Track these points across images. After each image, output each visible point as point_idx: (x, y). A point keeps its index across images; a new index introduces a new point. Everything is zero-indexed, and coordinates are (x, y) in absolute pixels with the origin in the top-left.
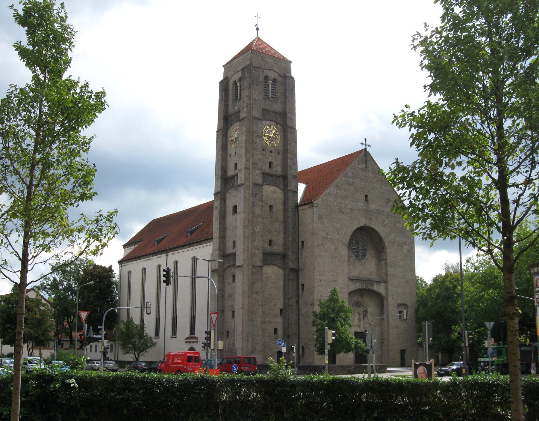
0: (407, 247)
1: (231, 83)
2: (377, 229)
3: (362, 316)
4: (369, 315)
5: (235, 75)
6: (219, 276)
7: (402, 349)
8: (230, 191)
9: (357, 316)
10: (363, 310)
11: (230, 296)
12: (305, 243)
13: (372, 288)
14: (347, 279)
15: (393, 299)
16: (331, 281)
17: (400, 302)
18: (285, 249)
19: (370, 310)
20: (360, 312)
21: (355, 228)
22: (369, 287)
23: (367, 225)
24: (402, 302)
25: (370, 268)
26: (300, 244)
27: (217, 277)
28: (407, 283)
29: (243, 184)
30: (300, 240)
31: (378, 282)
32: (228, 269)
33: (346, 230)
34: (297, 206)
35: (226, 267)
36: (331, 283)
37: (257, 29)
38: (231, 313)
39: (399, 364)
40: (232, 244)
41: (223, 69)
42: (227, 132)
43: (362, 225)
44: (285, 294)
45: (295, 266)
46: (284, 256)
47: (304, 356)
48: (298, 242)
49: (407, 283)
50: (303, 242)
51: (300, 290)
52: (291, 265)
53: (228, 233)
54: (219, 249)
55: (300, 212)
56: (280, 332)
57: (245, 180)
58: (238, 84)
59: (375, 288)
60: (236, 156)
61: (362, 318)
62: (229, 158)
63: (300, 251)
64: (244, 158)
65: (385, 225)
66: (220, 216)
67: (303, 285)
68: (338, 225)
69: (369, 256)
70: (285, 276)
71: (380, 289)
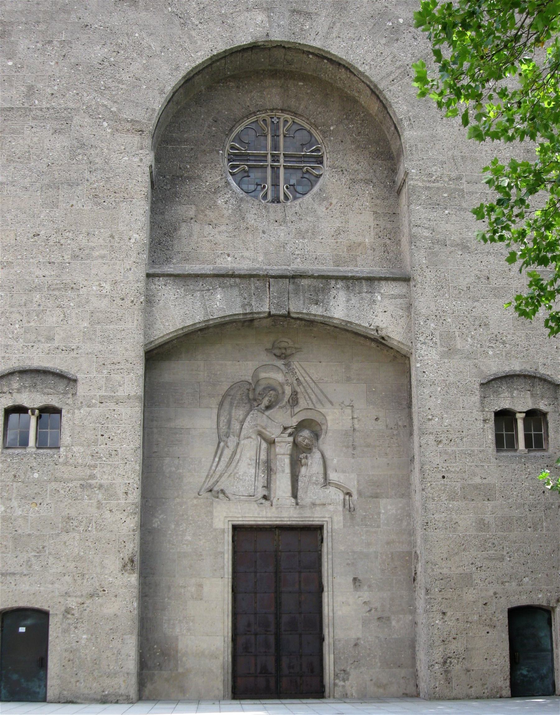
2: (337, 49)
3: (283, 449)
4: (329, 445)
7: (524, 601)
9: (249, 450)
10: (294, 422)
13: (316, 310)
15: (450, 352)
17: (495, 366)
19: (335, 420)
20: (274, 432)
21: (200, 57)
22: (297, 306)
23: (277, 36)
24: (516, 366)
25: (338, 232)
31: (351, 281)
33: (146, 68)
36: (37, 297)
39: (503, 681)
43: (244, 39)
59: (340, 307)
61: (283, 463)
68: (99, 52)
69: (329, 179)
71: (381, 314)
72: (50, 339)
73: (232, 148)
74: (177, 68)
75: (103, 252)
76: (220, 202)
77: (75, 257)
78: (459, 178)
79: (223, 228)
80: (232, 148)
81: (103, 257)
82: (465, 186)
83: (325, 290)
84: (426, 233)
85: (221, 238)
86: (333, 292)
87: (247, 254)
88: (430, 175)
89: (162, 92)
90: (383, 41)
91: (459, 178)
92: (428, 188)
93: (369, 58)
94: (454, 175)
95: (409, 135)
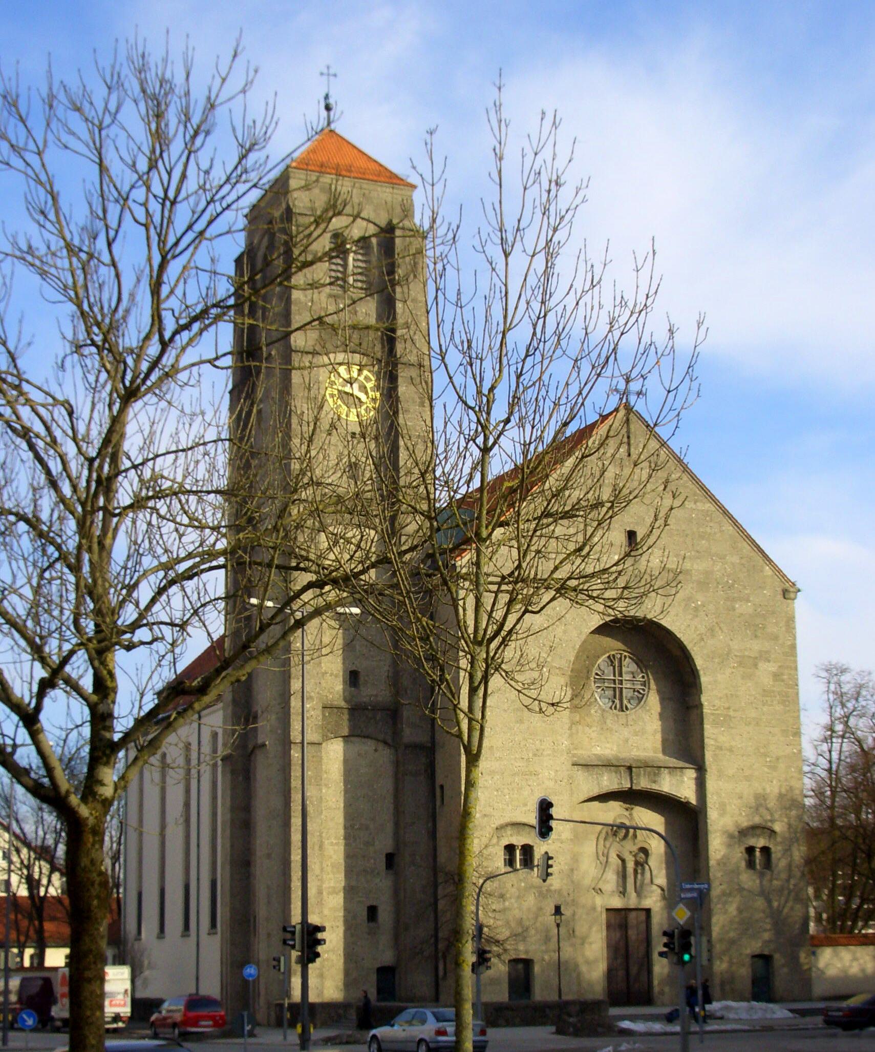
0: (772, 667)
13: (655, 787)
14: (568, 765)
16: (514, 775)
18: (397, 694)
28: (774, 768)
33: (565, 632)
37: (328, 108)
44: (398, 811)
45: (422, 738)
46: (393, 713)
49: (774, 768)
51: (438, 803)
52: (409, 734)
56: (385, 916)
65: (696, 609)
67: (442, 787)
70: (397, 764)
72: (525, 805)
73: (597, 674)
74: (581, 633)
75: (549, 752)
76: (592, 711)
77: (535, 755)
78: (729, 708)
79: (595, 729)
80: (597, 674)
81: (549, 755)
82: (731, 713)
83: (658, 774)
84: (712, 742)
85: (594, 735)
86: (663, 776)
87: (608, 745)
88: (714, 706)
89: (573, 647)
90: (690, 617)
91: (729, 708)
92: (713, 714)
93: (683, 627)
94: (727, 705)
95: (704, 680)
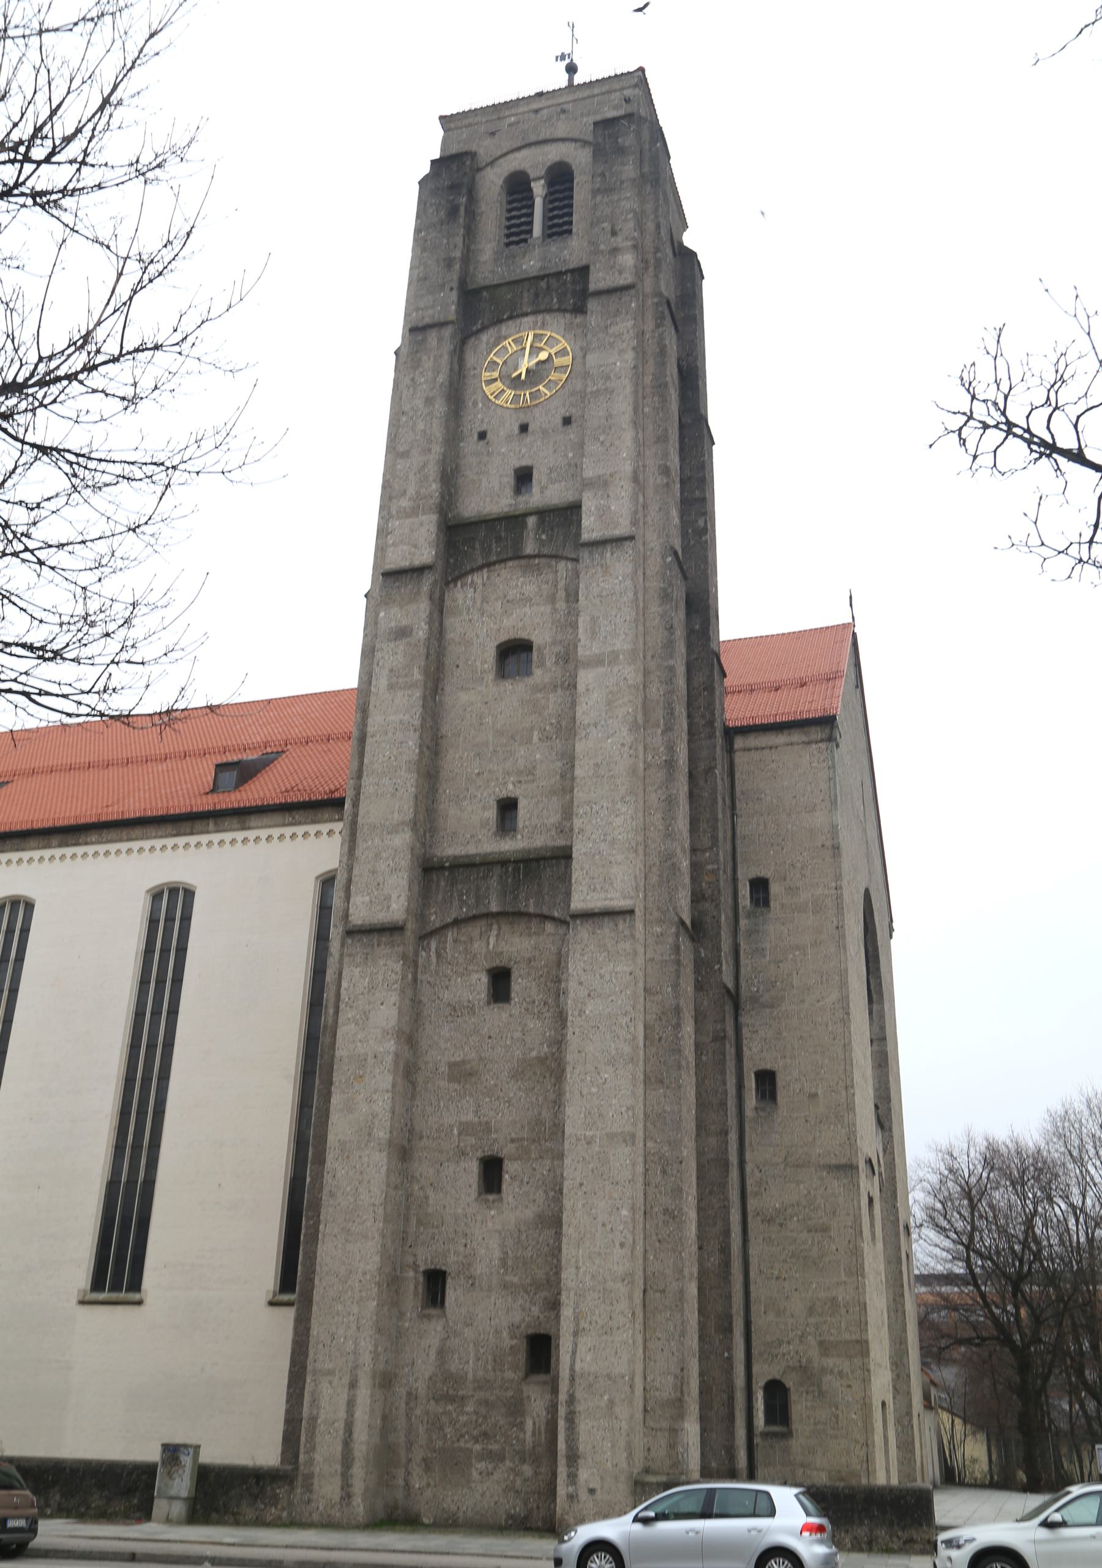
1: (492, 182)
5: (525, 152)
6: (404, 957)
8: (478, 578)
11: (461, 1073)
12: (775, 889)
26: (745, 891)
27: (398, 967)
29: (618, 541)
30: (746, 873)
32: (450, 935)
34: (731, 733)
35: (435, 920)
38: (474, 1167)
40: (492, 814)
41: (440, 133)
42: (464, 342)
47: (788, 1435)
48: (735, 880)
50: (760, 886)
53: (457, 761)
54: (414, 824)
55: (740, 759)
57: (634, 523)
58: (539, 189)
60: (528, 439)
62: (470, 445)
63: (743, 923)
64: (628, 436)
66: (426, 672)
